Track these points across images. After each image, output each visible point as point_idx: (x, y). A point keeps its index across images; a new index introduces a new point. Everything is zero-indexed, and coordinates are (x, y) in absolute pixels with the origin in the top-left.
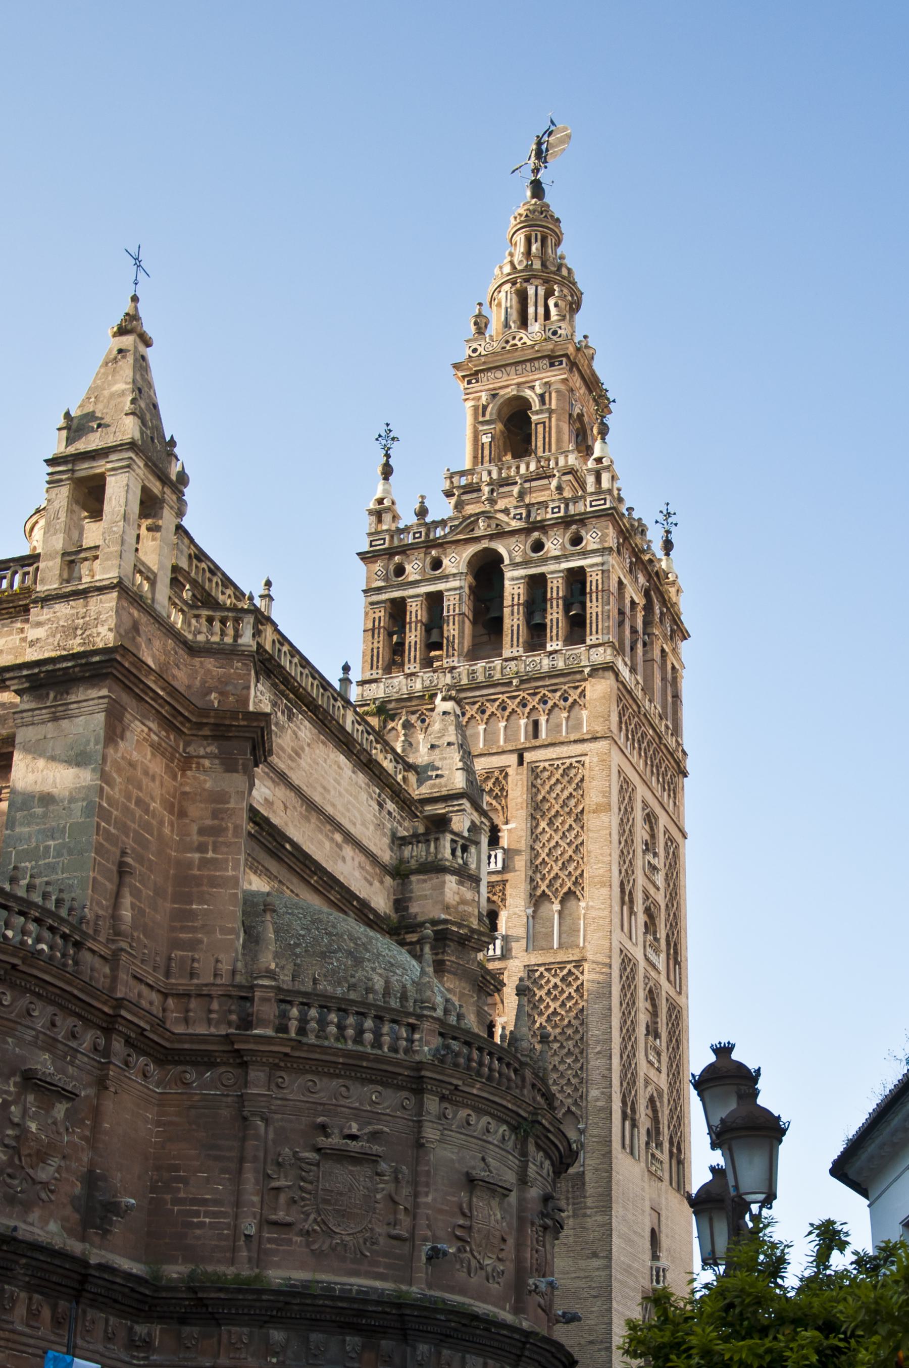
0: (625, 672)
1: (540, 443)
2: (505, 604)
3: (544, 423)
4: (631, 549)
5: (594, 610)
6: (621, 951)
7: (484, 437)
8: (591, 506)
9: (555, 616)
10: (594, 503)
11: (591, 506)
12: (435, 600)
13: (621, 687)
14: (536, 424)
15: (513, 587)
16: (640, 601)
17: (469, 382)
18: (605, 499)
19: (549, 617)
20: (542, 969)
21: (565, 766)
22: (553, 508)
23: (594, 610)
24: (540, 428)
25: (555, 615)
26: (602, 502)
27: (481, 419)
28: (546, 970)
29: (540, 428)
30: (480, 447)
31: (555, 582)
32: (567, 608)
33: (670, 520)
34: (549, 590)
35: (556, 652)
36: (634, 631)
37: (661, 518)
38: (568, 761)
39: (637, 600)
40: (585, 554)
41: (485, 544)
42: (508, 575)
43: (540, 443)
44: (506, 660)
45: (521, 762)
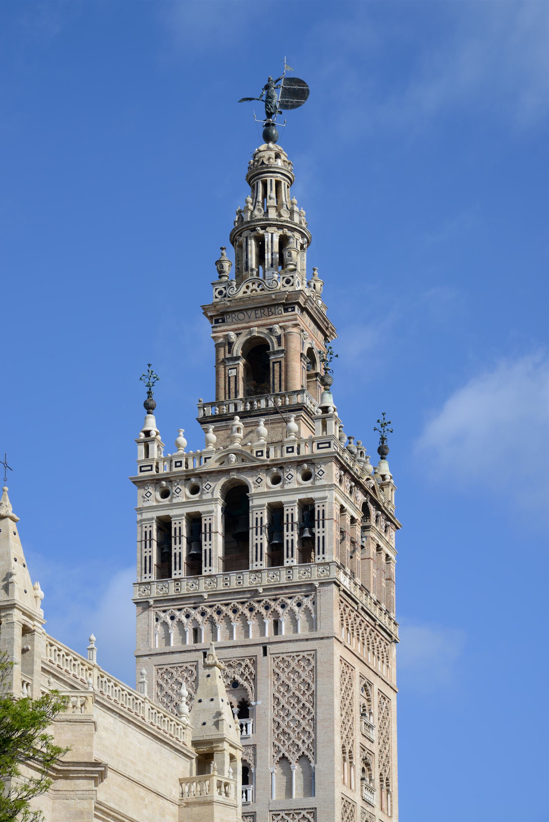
0: (345, 582)
1: (277, 381)
2: (251, 526)
3: (280, 362)
4: (350, 478)
5: (321, 535)
6: (343, 799)
7: (230, 371)
8: (318, 448)
9: (290, 538)
10: (320, 446)
11: (318, 448)
12: (195, 522)
13: (342, 593)
14: (274, 363)
15: (259, 514)
16: (358, 516)
17: (217, 322)
18: (329, 443)
19: (286, 538)
20: (282, 814)
21: (299, 658)
22: (288, 448)
23: (321, 535)
24: (277, 366)
25: (292, 536)
26: (327, 445)
27: (228, 356)
28: (286, 814)
29: (277, 366)
30: (227, 380)
31: (290, 510)
32: (301, 531)
33: (386, 427)
34: (285, 517)
35: (290, 567)
36: (353, 543)
37: (378, 426)
38: (302, 654)
39: (356, 517)
40: (314, 488)
41: (235, 476)
42: (254, 502)
43: (277, 381)
44: (252, 572)
45: (265, 654)
